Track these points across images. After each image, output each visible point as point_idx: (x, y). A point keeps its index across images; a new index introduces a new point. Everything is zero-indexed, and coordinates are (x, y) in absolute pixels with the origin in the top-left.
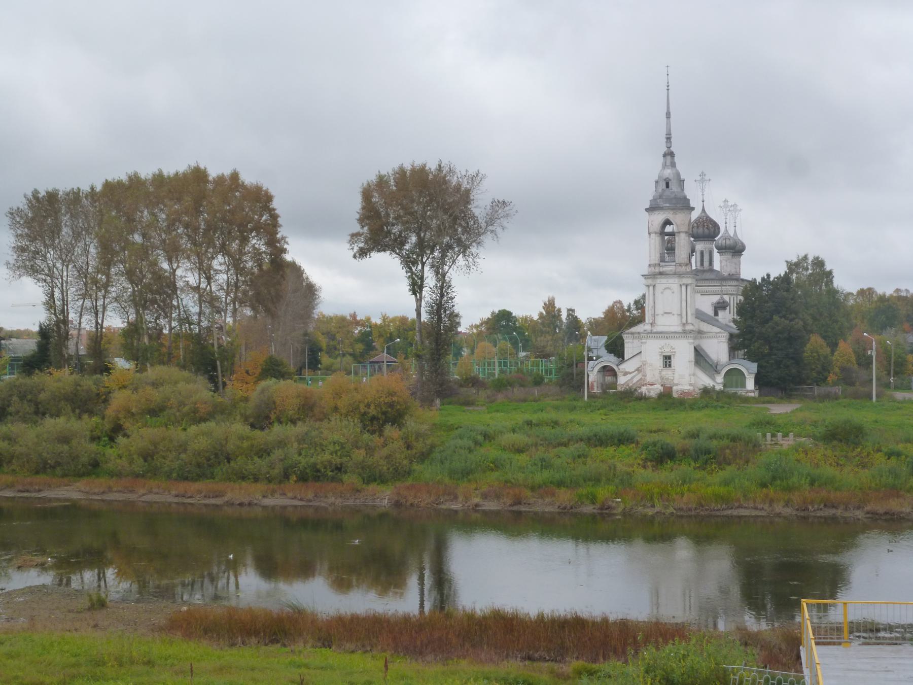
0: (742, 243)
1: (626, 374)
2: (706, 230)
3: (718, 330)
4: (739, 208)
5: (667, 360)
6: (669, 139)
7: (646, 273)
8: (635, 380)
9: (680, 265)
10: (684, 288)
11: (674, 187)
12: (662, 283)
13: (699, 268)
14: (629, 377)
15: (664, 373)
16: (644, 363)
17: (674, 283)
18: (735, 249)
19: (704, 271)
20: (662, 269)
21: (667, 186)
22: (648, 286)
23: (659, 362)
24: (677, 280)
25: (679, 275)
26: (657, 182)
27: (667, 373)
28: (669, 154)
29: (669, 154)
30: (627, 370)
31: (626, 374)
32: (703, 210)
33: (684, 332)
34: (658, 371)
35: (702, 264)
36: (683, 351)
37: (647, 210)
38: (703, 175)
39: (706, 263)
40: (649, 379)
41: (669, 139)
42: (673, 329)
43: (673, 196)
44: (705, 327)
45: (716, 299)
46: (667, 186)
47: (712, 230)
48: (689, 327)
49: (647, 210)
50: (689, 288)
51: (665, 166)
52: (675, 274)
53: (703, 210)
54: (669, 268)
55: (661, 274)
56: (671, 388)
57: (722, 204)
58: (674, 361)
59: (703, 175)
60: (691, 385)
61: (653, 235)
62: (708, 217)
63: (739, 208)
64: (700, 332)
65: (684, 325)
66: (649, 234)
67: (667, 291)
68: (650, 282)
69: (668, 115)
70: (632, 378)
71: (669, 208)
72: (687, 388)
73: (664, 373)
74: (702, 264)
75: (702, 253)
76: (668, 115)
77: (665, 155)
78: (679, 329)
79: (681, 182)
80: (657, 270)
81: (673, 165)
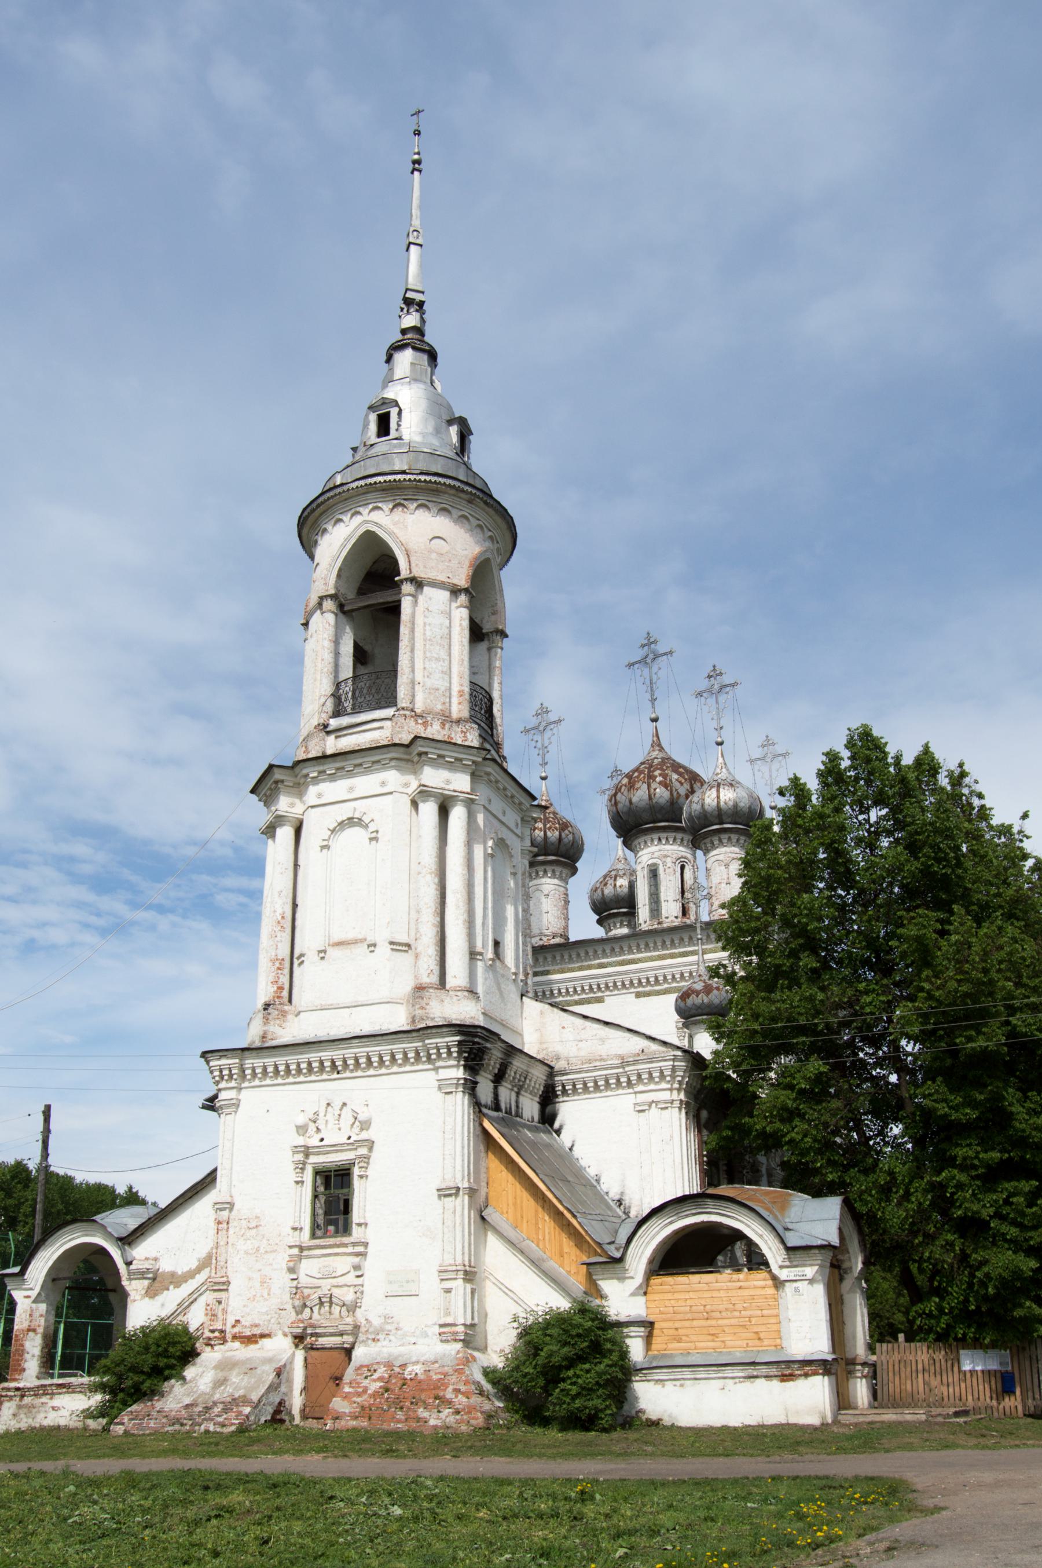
5: (334, 1196)
10: (429, 810)
23: (296, 1204)
24: (392, 778)
27: (328, 1266)
30: (166, 1266)
31: (157, 1281)
32: (657, 744)
34: (282, 1259)
40: (243, 1306)
50: (458, 815)
58: (366, 1198)
73: (309, 1268)
78: (398, 1019)
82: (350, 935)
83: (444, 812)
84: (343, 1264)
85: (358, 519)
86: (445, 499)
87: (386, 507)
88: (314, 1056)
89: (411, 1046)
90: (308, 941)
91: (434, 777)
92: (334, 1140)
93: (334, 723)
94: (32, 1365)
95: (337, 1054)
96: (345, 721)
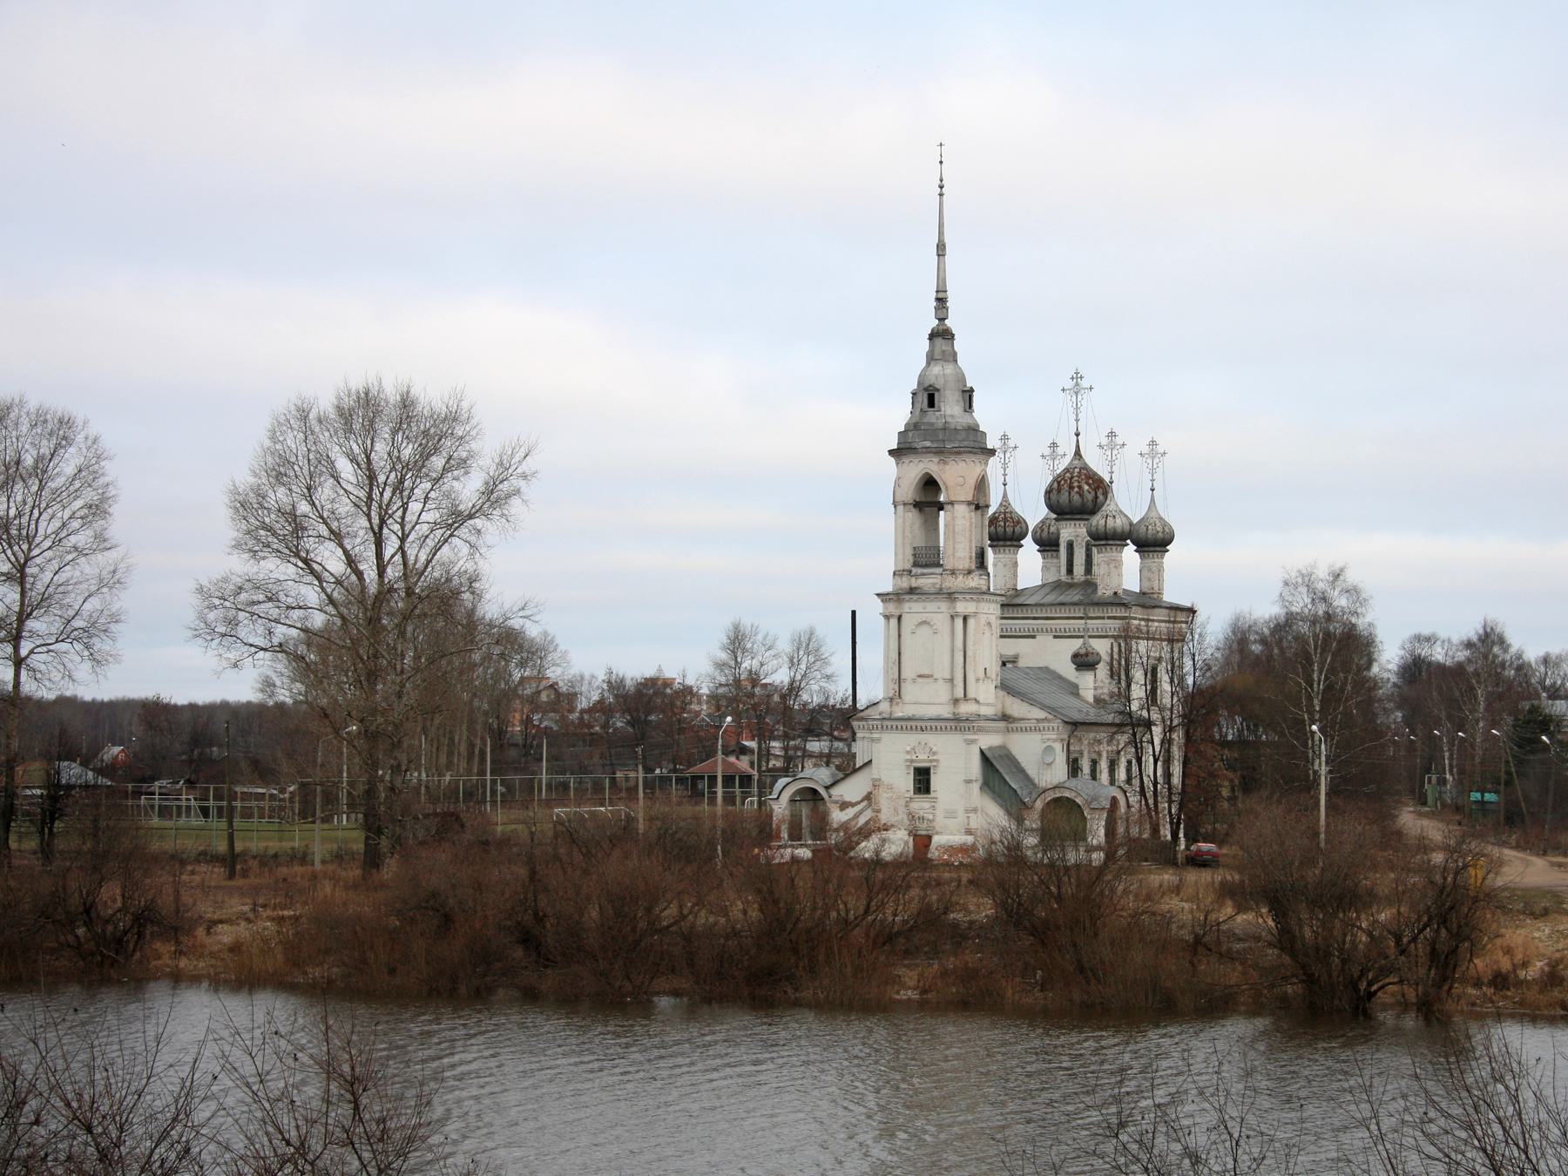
0: (1165, 524)
1: (844, 806)
2: (1076, 498)
3: (1042, 714)
4: (1160, 449)
5: (922, 780)
6: (941, 302)
7: (889, 588)
8: (862, 821)
9: (953, 572)
10: (959, 622)
11: (950, 408)
12: (914, 610)
13: (1064, 578)
14: (850, 812)
15: (914, 806)
16: (876, 784)
17: (937, 612)
18: (1153, 543)
19: (1070, 586)
20: (914, 583)
21: (931, 403)
22: (887, 617)
23: (907, 782)
24: (944, 606)
25: (951, 596)
26: (914, 394)
27: (921, 805)
28: (941, 335)
29: (941, 335)
30: (847, 799)
31: (844, 806)
32: (1078, 453)
33: (957, 719)
34: (903, 802)
35: (1070, 571)
36: (957, 764)
37: (891, 452)
38: (1077, 377)
39: (1079, 569)
41: (941, 302)
42: (932, 711)
43: (940, 426)
44: (1017, 708)
45: (1075, 645)
46: (931, 403)
47: (1090, 497)
48: (966, 709)
49: (891, 452)
50: (971, 622)
51: (931, 358)
52: (940, 592)
53: (1078, 453)
54: (928, 581)
55: (912, 591)
56: (929, 838)
57: (1105, 441)
58: (936, 781)
59: (1077, 377)
60: (969, 832)
61: (900, 508)
62: (1085, 467)
63: (1160, 449)
64: (1005, 718)
65: (956, 701)
66: (895, 504)
67: (925, 628)
68: (892, 608)
69: (941, 249)
70: (857, 816)
71: (927, 451)
72: (959, 839)
73: (914, 806)
74: (1070, 571)
75: (1070, 546)
76: (941, 249)
77: (932, 336)
78: (946, 711)
79: (968, 395)
80: (905, 583)
81: (953, 357)
82: (926, 672)
83: (965, 619)
84: (927, 805)
85: (921, 466)
86: (964, 457)
87: (936, 460)
88: (913, 724)
89: (953, 724)
90: (907, 673)
91: (962, 607)
92: (922, 760)
93: (914, 570)
94: (785, 835)
95: (923, 724)
96: (920, 571)
